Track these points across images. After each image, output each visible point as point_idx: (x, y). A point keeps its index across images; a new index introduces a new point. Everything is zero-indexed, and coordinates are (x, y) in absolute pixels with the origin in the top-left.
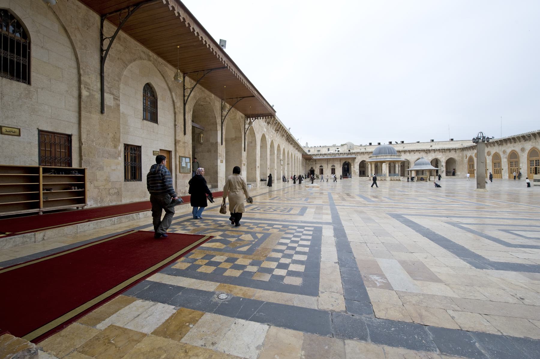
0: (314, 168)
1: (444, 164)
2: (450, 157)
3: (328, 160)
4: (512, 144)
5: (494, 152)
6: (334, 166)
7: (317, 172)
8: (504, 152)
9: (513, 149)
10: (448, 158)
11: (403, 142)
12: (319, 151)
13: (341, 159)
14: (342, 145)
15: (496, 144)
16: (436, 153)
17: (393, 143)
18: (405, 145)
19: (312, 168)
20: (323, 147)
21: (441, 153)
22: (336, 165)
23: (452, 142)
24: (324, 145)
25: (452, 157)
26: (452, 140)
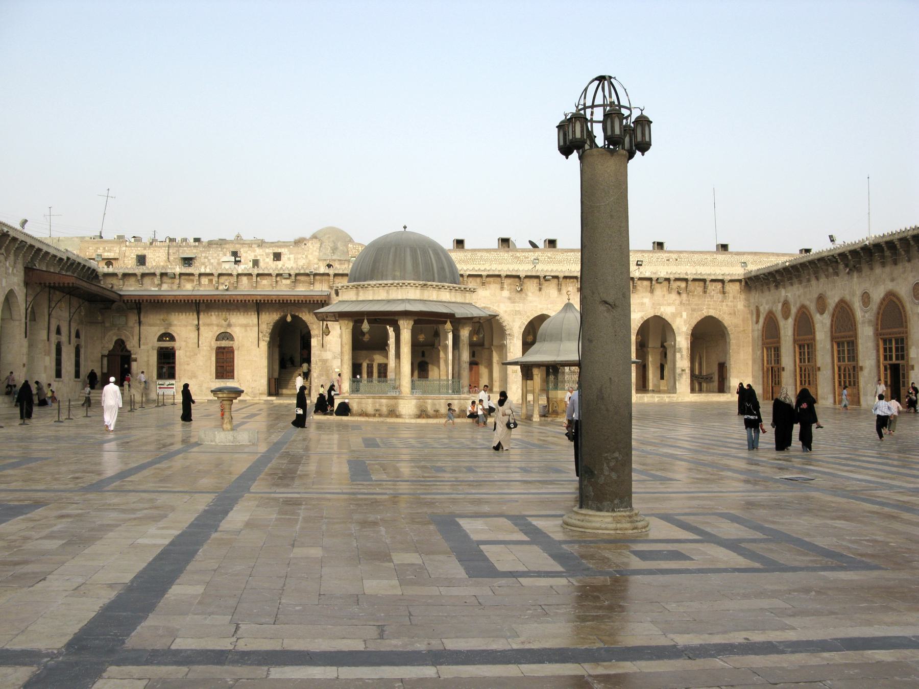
0: (131, 345)
1: (683, 342)
2: (705, 313)
3: (198, 306)
4: (888, 269)
5: (837, 300)
6: (225, 336)
7: (145, 360)
8: (866, 298)
9: (890, 286)
10: (697, 317)
11: (552, 243)
12: (188, 261)
13: (259, 306)
14: (299, 242)
15: (841, 266)
16: (660, 291)
17: (521, 242)
18: (560, 256)
19: (120, 344)
20: (210, 243)
21: (674, 296)
22: (236, 332)
23: (721, 257)
24: (215, 237)
25: (712, 313)
26: (724, 247)
